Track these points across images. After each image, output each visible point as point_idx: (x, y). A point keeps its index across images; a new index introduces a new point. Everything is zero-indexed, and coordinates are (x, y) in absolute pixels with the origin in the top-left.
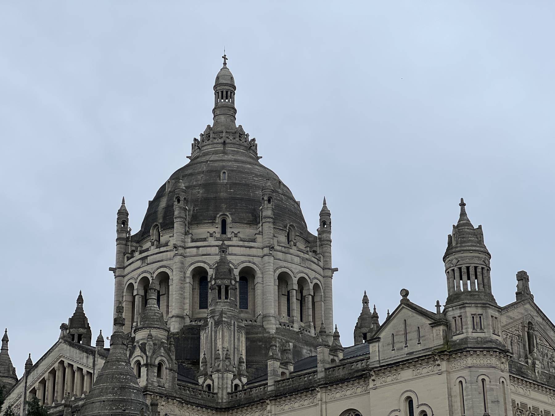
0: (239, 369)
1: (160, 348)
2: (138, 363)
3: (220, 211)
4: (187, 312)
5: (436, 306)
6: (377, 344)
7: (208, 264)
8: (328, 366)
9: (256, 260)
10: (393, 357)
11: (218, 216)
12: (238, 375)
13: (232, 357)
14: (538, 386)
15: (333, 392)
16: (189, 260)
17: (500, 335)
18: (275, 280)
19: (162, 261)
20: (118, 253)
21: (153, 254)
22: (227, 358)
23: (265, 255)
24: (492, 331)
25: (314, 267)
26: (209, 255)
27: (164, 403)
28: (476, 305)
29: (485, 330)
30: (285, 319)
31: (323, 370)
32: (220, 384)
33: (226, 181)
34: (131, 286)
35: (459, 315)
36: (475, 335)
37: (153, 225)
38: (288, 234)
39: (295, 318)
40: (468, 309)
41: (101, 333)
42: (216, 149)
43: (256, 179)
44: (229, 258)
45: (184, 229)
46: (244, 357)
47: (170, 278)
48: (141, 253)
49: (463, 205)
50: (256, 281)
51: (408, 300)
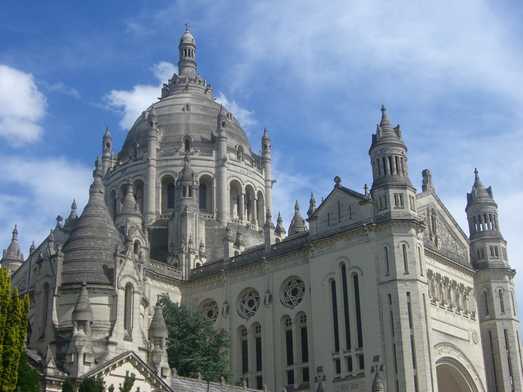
0: (200, 251)
1: (135, 230)
5: (364, 188)
6: (315, 222)
10: (329, 231)
13: (194, 241)
17: (416, 210)
19: (138, 171)
21: (131, 166)
30: (236, 216)
34: (113, 192)
35: (383, 195)
36: (396, 210)
38: (237, 153)
46: (204, 242)
47: (145, 184)
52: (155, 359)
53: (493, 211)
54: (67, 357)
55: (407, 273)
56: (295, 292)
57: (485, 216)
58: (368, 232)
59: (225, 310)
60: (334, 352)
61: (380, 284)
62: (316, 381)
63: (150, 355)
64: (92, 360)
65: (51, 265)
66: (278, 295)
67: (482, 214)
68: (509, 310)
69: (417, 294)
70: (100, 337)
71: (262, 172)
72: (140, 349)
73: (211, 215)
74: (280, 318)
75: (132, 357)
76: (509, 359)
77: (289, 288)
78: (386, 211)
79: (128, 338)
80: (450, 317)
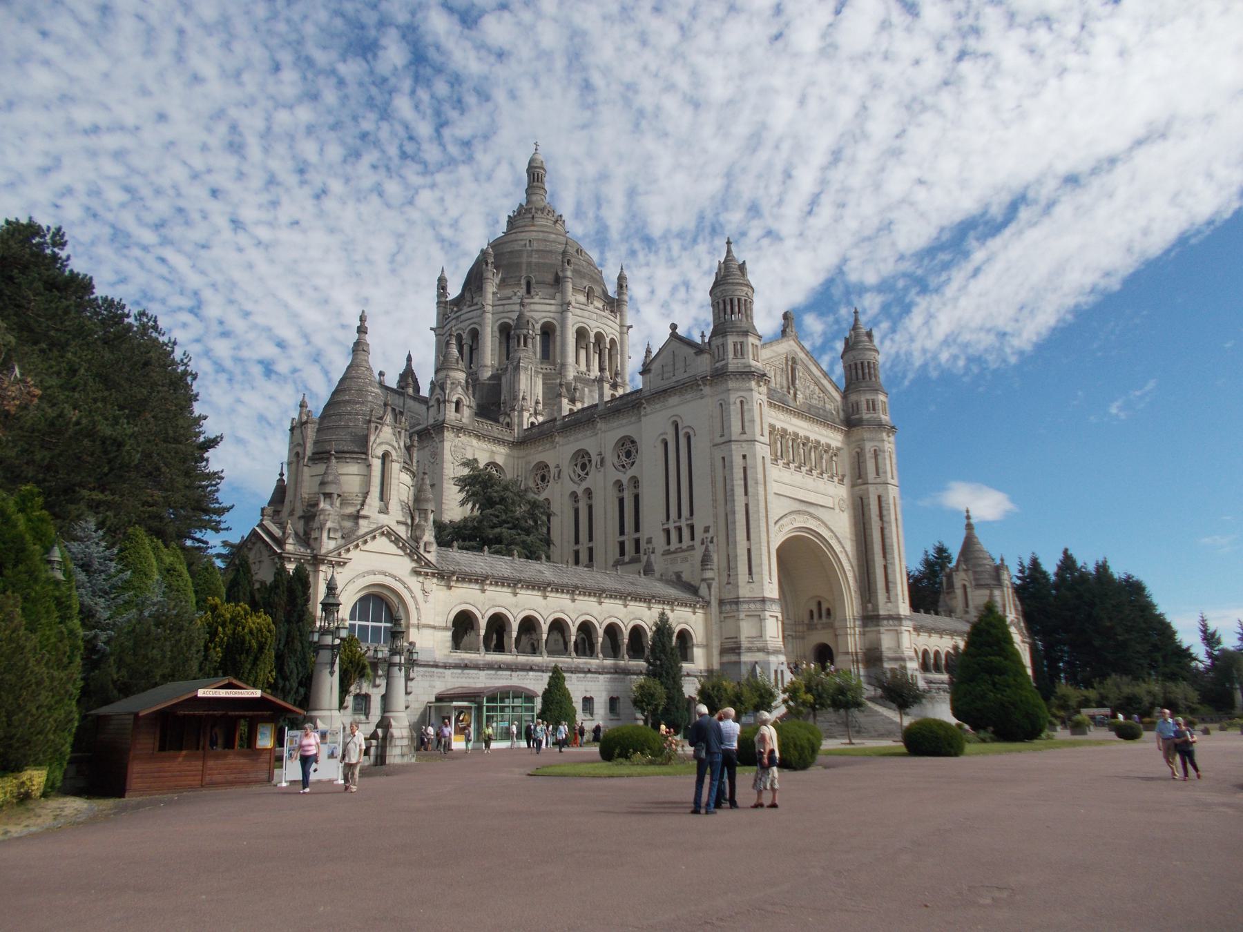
1: (457, 387)
13: (528, 398)
19: (472, 318)
30: (583, 368)
36: (735, 361)
46: (540, 399)
52: (418, 533)
53: (872, 357)
54: (312, 533)
55: (744, 433)
56: (628, 454)
57: (862, 363)
58: (702, 387)
59: (556, 475)
60: (665, 521)
61: (714, 446)
62: (645, 554)
63: (414, 528)
64: (339, 535)
65: (302, 433)
66: (610, 458)
67: (859, 362)
68: (885, 472)
69: (754, 456)
70: (351, 510)
72: (398, 522)
73: (552, 367)
74: (612, 483)
75: (388, 532)
76: (882, 529)
78: (723, 363)
79: (384, 510)
80: (810, 482)
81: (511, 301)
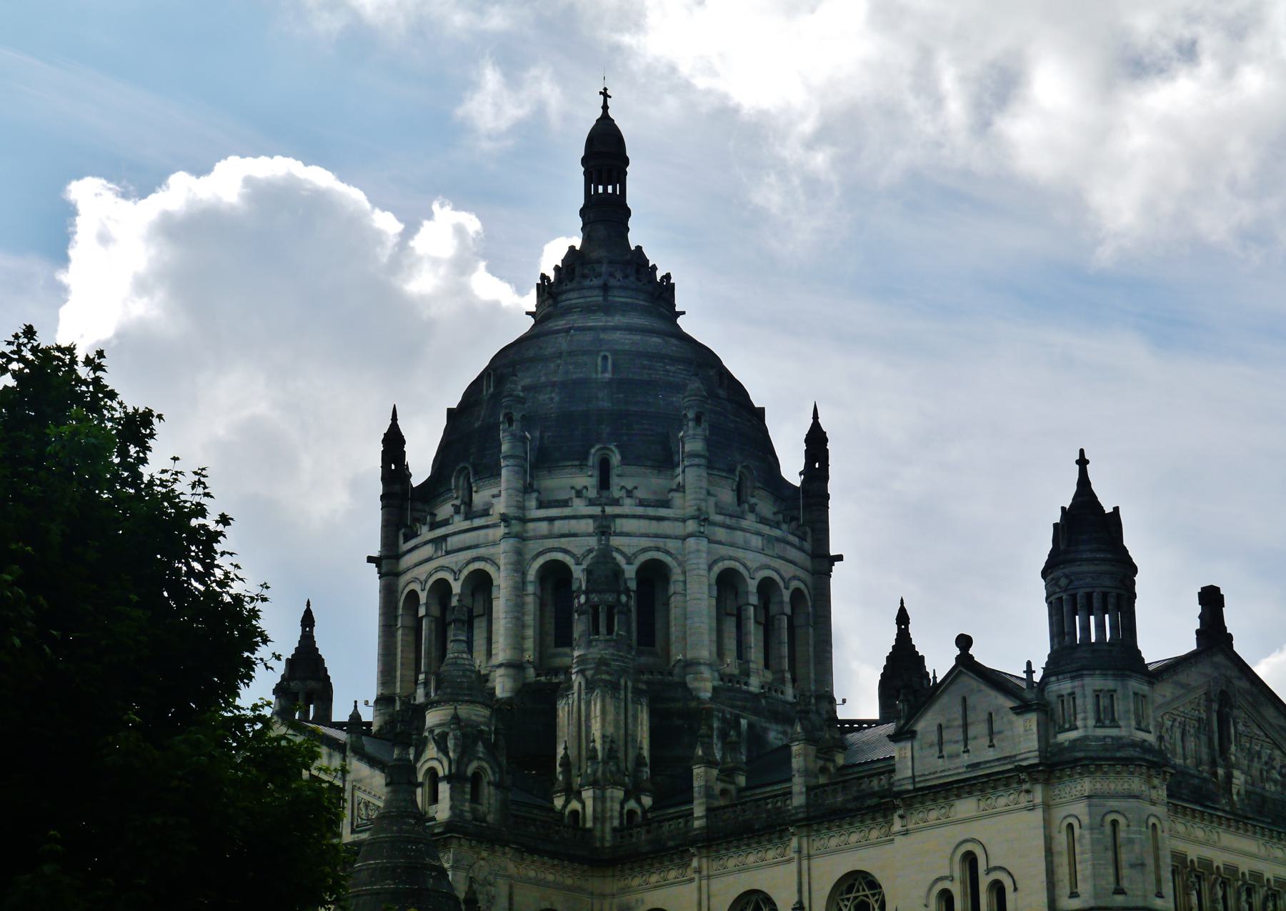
2: (432, 772)
3: (598, 441)
4: (529, 656)
6: (909, 745)
7: (573, 556)
8: (813, 782)
9: (672, 545)
10: (941, 772)
11: (593, 451)
12: (633, 792)
13: (621, 755)
14: (1237, 822)
15: (822, 836)
16: (534, 547)
17: (1151, 729)
18: (710, 585)
19: (476, 546)
20: (387, 525)
22: (611, 754)
23: (690, 535)
24: (1133, 723)
25: (793, 554)
26: (575, 535)
27: (484, 854)
28: (1104, 672)
29: (1121, 723)
30: (731, 663)
31: (804, 790)
32: (599, 809)
33: (608, 375)
34: (413, 595)
35: (1069, 691)
36: (1100, 732)
37: (458, 468)
39: (752, 665)
40: (1087, 681)
41: (356, 706)
42: (588, 300)
43: (672, 369)
44: (615, 541)
45: (522, 482)
46: (646, 753)
47: (495, 583)
48: (434, 526)
49: (1082, 462)
50: (672, 590)
51: (971, 657)
71: (805, 533)
77: (848, 899)
78: (1073, 735)
81: (567, 511)
